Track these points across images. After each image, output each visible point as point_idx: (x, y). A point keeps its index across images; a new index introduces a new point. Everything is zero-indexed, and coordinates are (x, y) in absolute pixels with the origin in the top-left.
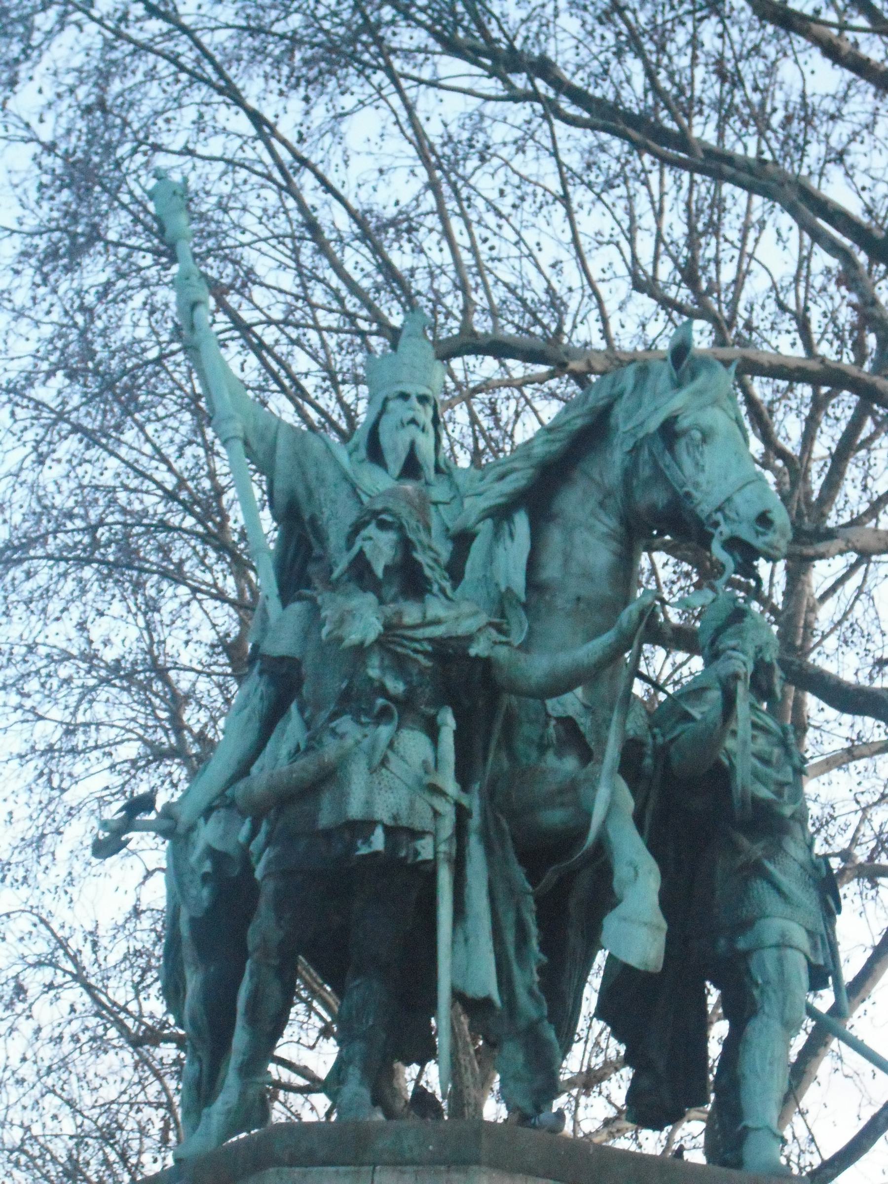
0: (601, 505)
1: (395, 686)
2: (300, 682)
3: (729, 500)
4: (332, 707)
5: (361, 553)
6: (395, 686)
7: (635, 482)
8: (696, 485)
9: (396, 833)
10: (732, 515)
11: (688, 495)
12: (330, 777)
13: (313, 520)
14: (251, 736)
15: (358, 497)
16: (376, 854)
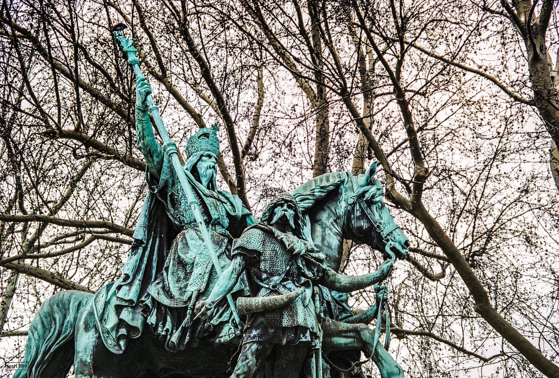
0: (335, 221)
1: (310, 274)
2: (259, 262)
3: (391, 232)
4: (283, 276)
5: (284, 216)
6: (310, 274)
7: (352, 216)
8: (380, 223)
9: (314, 335)
10: (393, 239)
11: (378, 226)
12: (289, 305)
13: (172, 195)
14: (233, 281)
16: (308, 341)
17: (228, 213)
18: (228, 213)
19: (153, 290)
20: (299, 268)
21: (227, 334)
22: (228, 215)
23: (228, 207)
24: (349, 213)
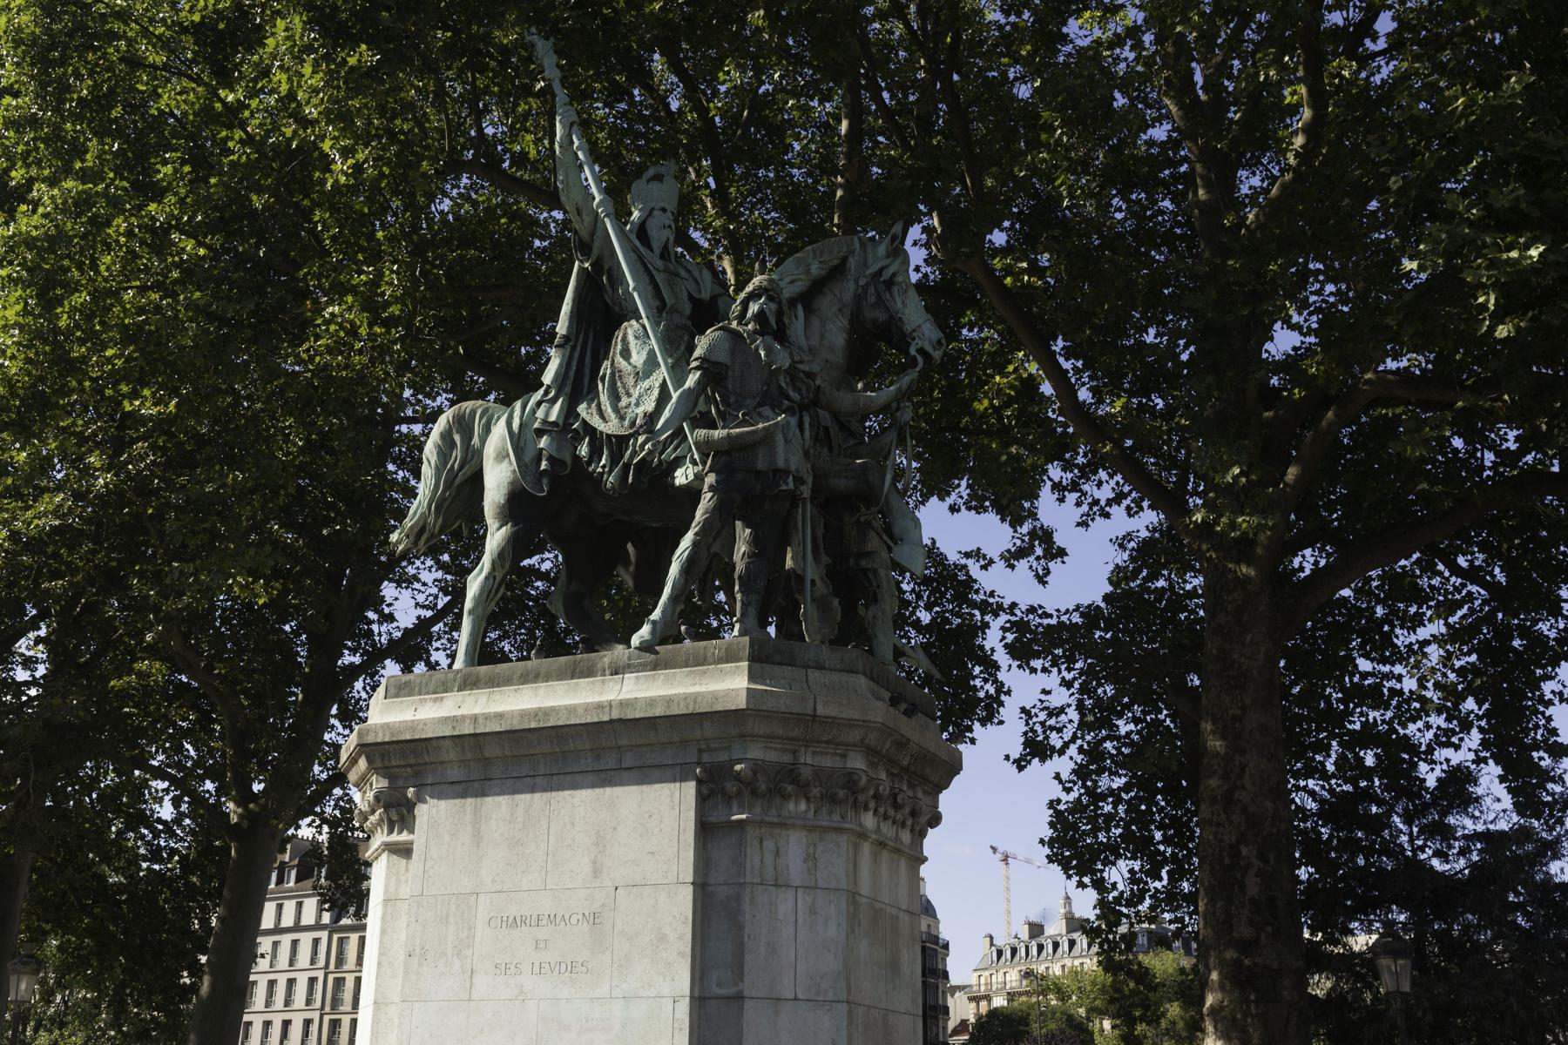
9: (799, 480)
15: (644, 265)
17: (690, 295)
18: (690, 295)
19: (582, 409)
20: (780, 388)
21: (682, 476)
22: (691, 297)
23: (692, 287)
24: (859, 299)
